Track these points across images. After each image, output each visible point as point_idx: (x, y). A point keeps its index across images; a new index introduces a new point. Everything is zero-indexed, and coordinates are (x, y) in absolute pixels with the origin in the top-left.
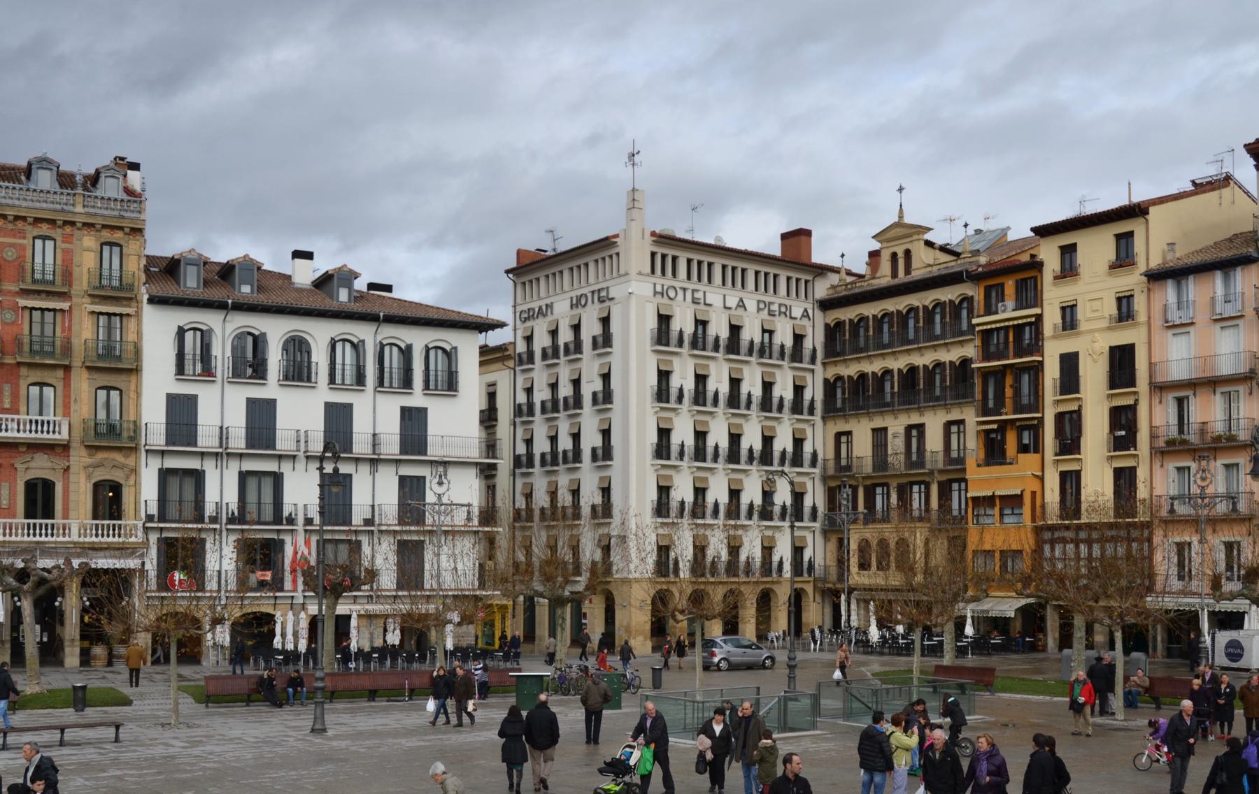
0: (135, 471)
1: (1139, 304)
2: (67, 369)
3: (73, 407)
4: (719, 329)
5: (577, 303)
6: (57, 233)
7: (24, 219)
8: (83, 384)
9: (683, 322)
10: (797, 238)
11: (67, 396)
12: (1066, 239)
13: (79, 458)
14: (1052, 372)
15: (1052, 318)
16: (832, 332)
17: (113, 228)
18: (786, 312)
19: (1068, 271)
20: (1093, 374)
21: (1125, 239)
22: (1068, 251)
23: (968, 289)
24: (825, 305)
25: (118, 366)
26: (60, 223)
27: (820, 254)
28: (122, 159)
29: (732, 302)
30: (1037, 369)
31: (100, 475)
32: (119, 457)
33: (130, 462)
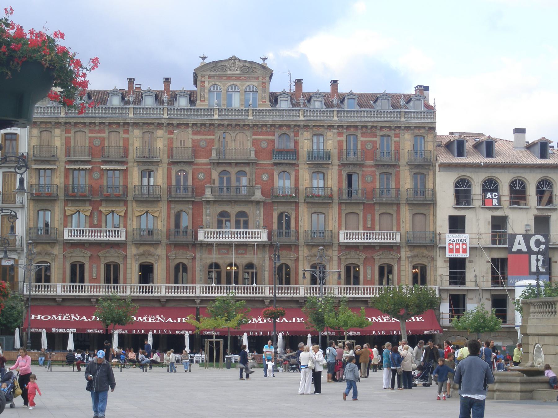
0: (433, 259)
2: (398, 205)
3: (402, 225)
6: (392, 133)
7: (376, 127)
8: (406, 213)
11: (398, 219)
13: (405, 253)
17: (419, 128)
25: (424, 203)
26: (393, 128)
28: (421, 86)
31: (417, 261)
32: (425, 252)
33: (431, 254)
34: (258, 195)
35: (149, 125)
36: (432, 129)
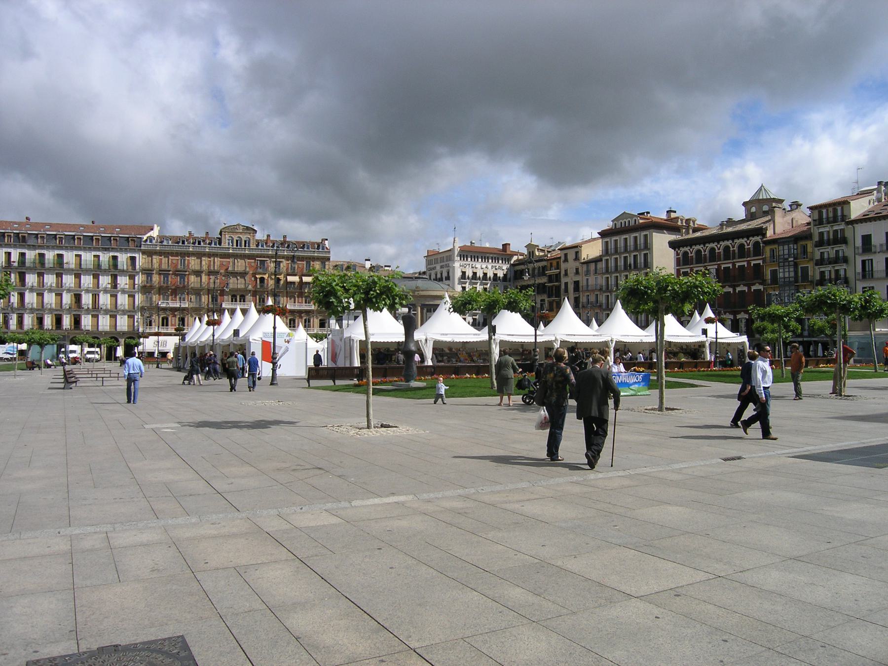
1: (580, 271)
4: (480, 274)
5: (442, 267)
9: (469, 273)
10: (505, 246)
12: (565, 252)
14: (563, 287)
15: (563, 273)
16: (516, 272)
18: (500, 268)
19: (566, 260)
20: (571, 287)
21: (577, 253)
22: (566, 255)
23: (544, 263)
24: (513, 265)
27: (513, 248)
29: (484, 266)
30: (559, 287)
34: (250, 287)
35: (199, 255)
36: (329, 259)
